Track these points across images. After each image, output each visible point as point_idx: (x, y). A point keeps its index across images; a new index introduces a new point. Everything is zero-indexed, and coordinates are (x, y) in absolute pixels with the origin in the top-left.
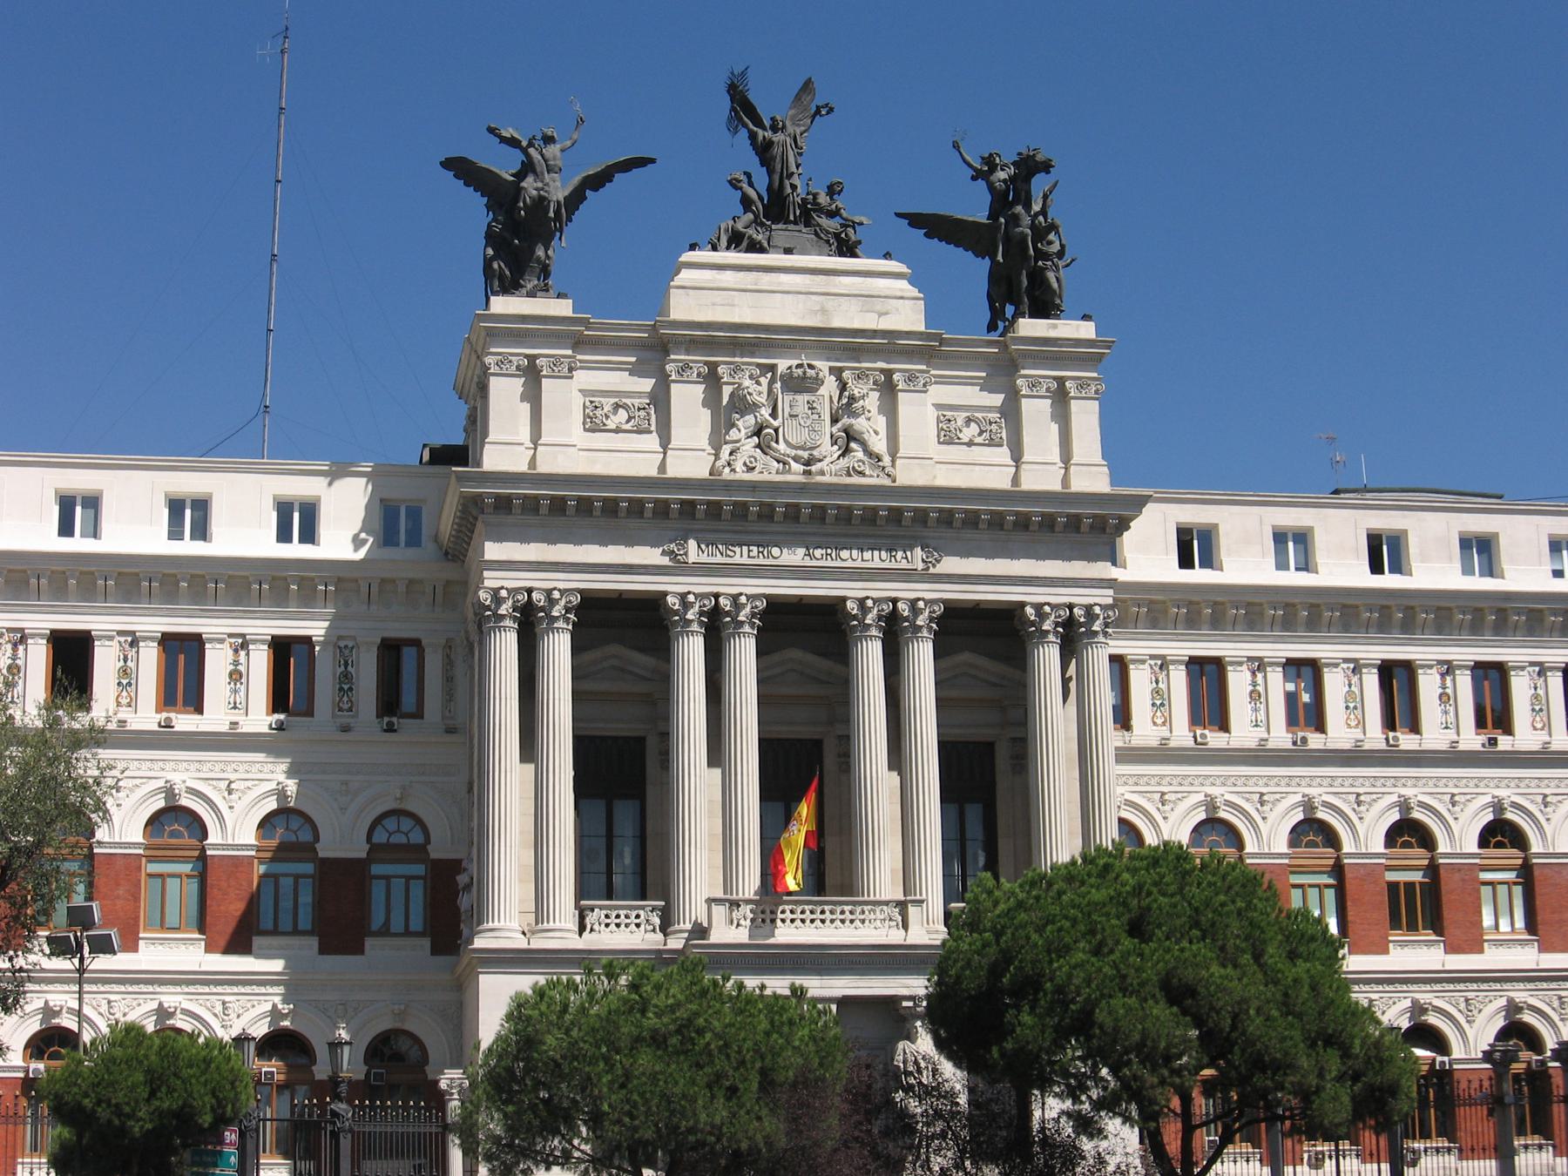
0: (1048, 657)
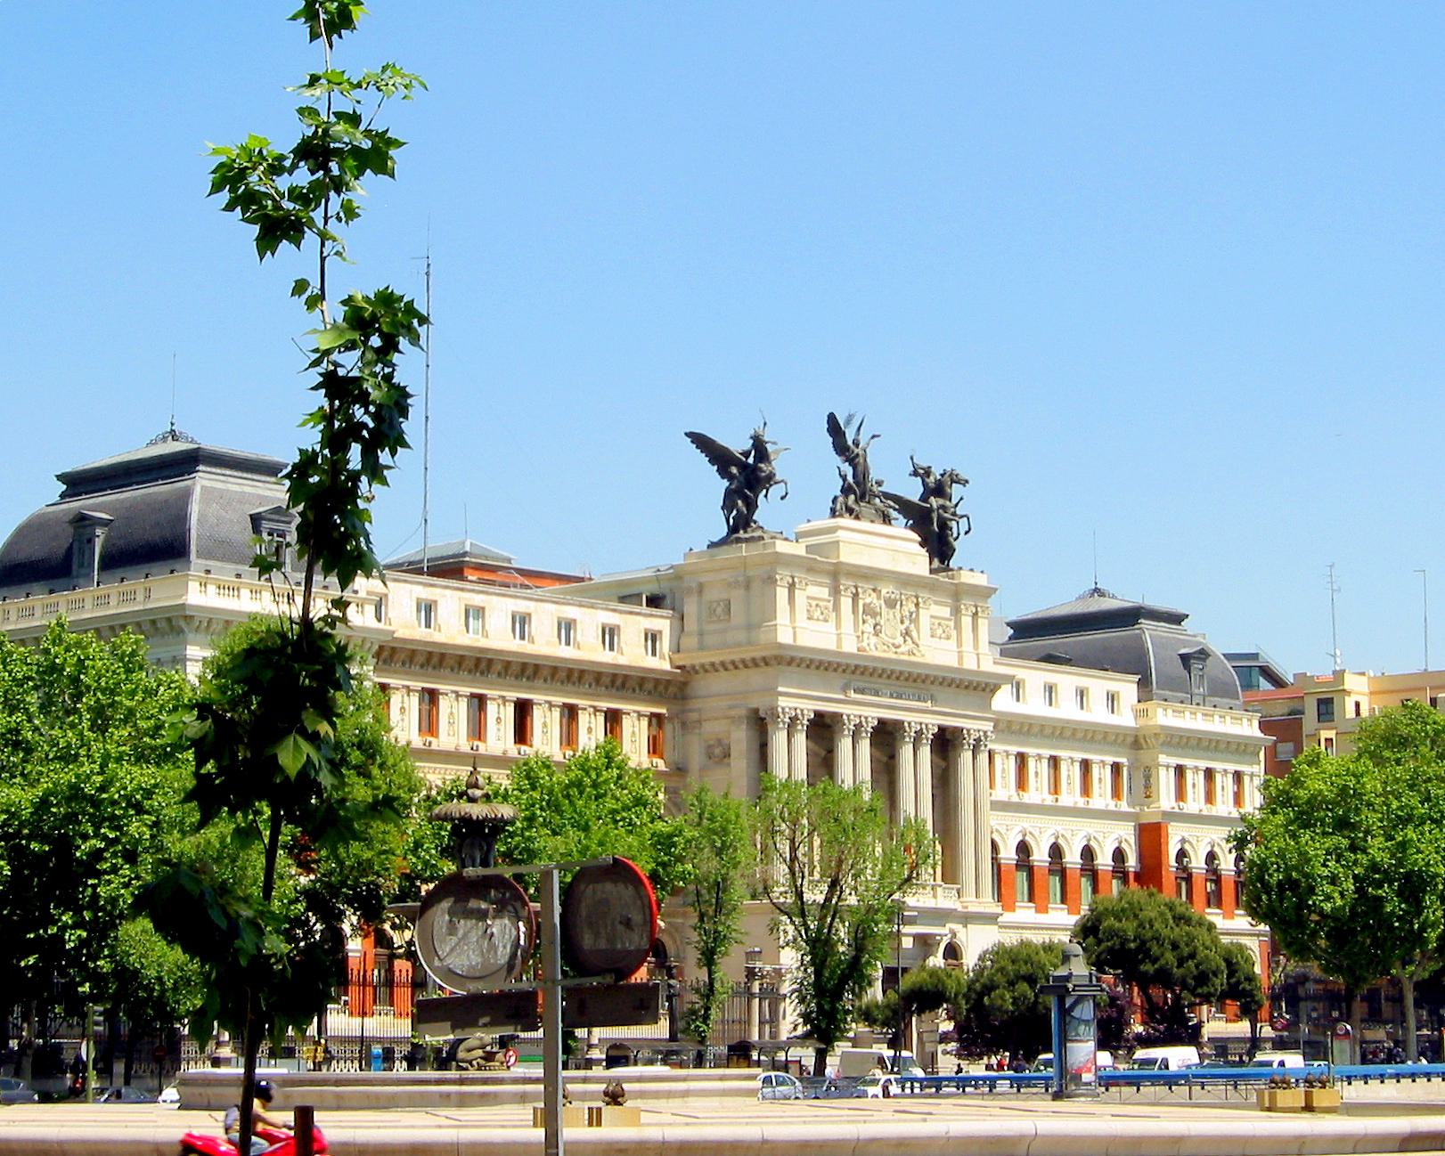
0: (966, 756)
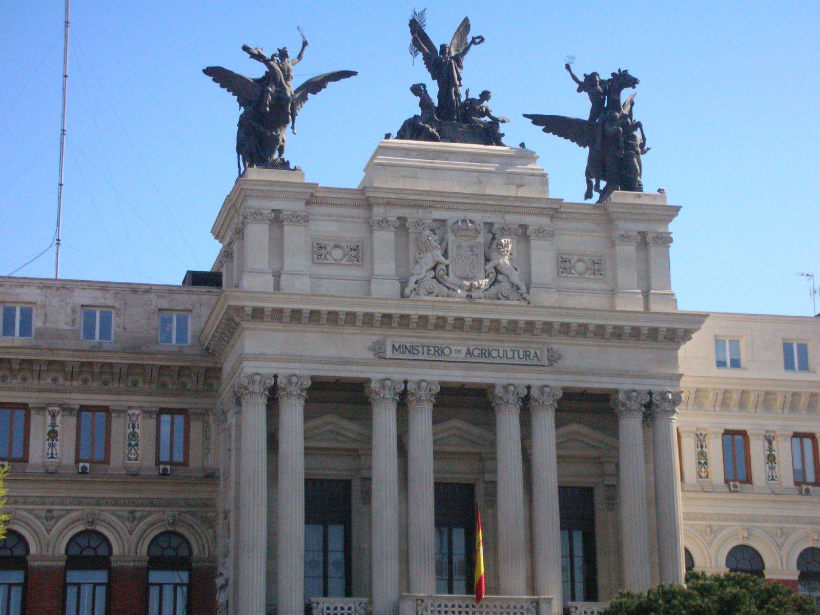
0: (631, 426)
